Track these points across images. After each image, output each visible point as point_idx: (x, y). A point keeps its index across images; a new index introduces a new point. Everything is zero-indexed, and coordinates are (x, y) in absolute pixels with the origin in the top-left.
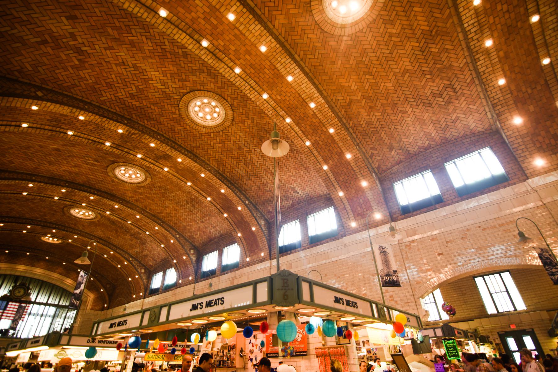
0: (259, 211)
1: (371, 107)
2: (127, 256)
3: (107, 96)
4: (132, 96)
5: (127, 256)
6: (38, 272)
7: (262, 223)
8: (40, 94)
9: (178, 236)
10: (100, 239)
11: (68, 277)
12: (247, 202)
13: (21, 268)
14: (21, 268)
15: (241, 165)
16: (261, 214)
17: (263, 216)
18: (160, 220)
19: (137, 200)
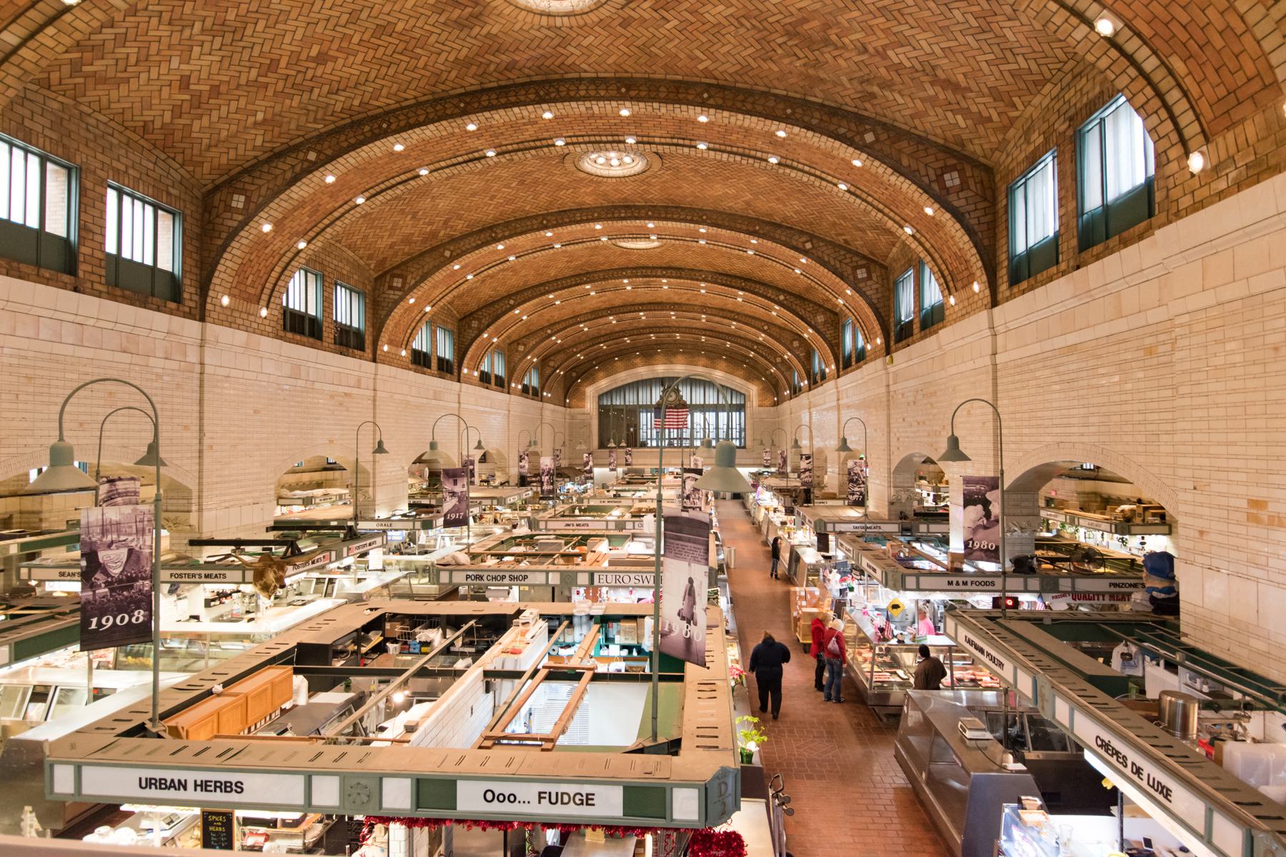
0: (811, 302)
1: (777, 199)
2: (748, 344)
3: (553, 273)
4: (567, 262)
5: (748, 344)
6: (679, 369)
7: (820, 318)
8: (512, 302)
9: (766, 328)
10: (705, 330)
11: (714, 368)
12: (782, 297)
13: (661, 369)
14: (661, 369)
15: (734, 260)
16: (815, 303)
17: (820, 306)
18: (733, 312)
19: (689, 300)
